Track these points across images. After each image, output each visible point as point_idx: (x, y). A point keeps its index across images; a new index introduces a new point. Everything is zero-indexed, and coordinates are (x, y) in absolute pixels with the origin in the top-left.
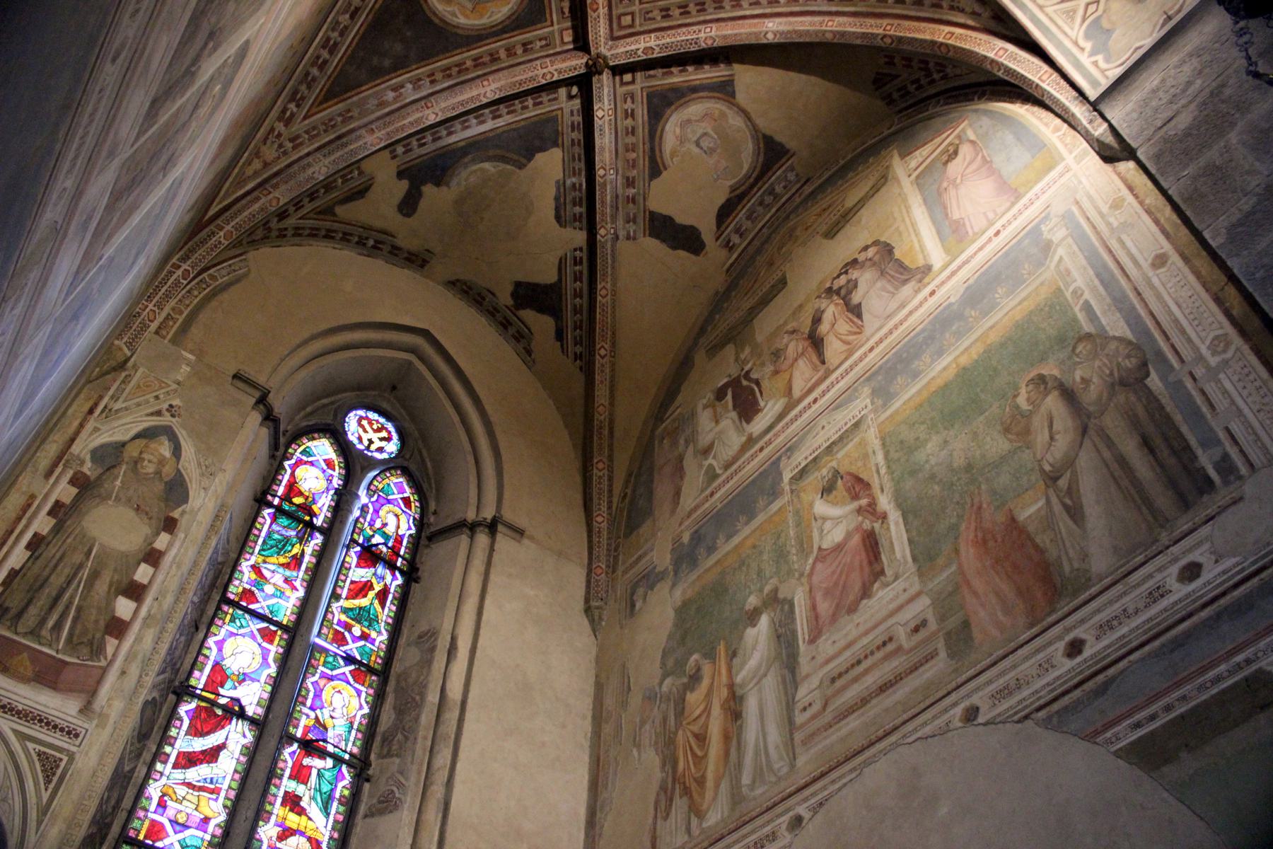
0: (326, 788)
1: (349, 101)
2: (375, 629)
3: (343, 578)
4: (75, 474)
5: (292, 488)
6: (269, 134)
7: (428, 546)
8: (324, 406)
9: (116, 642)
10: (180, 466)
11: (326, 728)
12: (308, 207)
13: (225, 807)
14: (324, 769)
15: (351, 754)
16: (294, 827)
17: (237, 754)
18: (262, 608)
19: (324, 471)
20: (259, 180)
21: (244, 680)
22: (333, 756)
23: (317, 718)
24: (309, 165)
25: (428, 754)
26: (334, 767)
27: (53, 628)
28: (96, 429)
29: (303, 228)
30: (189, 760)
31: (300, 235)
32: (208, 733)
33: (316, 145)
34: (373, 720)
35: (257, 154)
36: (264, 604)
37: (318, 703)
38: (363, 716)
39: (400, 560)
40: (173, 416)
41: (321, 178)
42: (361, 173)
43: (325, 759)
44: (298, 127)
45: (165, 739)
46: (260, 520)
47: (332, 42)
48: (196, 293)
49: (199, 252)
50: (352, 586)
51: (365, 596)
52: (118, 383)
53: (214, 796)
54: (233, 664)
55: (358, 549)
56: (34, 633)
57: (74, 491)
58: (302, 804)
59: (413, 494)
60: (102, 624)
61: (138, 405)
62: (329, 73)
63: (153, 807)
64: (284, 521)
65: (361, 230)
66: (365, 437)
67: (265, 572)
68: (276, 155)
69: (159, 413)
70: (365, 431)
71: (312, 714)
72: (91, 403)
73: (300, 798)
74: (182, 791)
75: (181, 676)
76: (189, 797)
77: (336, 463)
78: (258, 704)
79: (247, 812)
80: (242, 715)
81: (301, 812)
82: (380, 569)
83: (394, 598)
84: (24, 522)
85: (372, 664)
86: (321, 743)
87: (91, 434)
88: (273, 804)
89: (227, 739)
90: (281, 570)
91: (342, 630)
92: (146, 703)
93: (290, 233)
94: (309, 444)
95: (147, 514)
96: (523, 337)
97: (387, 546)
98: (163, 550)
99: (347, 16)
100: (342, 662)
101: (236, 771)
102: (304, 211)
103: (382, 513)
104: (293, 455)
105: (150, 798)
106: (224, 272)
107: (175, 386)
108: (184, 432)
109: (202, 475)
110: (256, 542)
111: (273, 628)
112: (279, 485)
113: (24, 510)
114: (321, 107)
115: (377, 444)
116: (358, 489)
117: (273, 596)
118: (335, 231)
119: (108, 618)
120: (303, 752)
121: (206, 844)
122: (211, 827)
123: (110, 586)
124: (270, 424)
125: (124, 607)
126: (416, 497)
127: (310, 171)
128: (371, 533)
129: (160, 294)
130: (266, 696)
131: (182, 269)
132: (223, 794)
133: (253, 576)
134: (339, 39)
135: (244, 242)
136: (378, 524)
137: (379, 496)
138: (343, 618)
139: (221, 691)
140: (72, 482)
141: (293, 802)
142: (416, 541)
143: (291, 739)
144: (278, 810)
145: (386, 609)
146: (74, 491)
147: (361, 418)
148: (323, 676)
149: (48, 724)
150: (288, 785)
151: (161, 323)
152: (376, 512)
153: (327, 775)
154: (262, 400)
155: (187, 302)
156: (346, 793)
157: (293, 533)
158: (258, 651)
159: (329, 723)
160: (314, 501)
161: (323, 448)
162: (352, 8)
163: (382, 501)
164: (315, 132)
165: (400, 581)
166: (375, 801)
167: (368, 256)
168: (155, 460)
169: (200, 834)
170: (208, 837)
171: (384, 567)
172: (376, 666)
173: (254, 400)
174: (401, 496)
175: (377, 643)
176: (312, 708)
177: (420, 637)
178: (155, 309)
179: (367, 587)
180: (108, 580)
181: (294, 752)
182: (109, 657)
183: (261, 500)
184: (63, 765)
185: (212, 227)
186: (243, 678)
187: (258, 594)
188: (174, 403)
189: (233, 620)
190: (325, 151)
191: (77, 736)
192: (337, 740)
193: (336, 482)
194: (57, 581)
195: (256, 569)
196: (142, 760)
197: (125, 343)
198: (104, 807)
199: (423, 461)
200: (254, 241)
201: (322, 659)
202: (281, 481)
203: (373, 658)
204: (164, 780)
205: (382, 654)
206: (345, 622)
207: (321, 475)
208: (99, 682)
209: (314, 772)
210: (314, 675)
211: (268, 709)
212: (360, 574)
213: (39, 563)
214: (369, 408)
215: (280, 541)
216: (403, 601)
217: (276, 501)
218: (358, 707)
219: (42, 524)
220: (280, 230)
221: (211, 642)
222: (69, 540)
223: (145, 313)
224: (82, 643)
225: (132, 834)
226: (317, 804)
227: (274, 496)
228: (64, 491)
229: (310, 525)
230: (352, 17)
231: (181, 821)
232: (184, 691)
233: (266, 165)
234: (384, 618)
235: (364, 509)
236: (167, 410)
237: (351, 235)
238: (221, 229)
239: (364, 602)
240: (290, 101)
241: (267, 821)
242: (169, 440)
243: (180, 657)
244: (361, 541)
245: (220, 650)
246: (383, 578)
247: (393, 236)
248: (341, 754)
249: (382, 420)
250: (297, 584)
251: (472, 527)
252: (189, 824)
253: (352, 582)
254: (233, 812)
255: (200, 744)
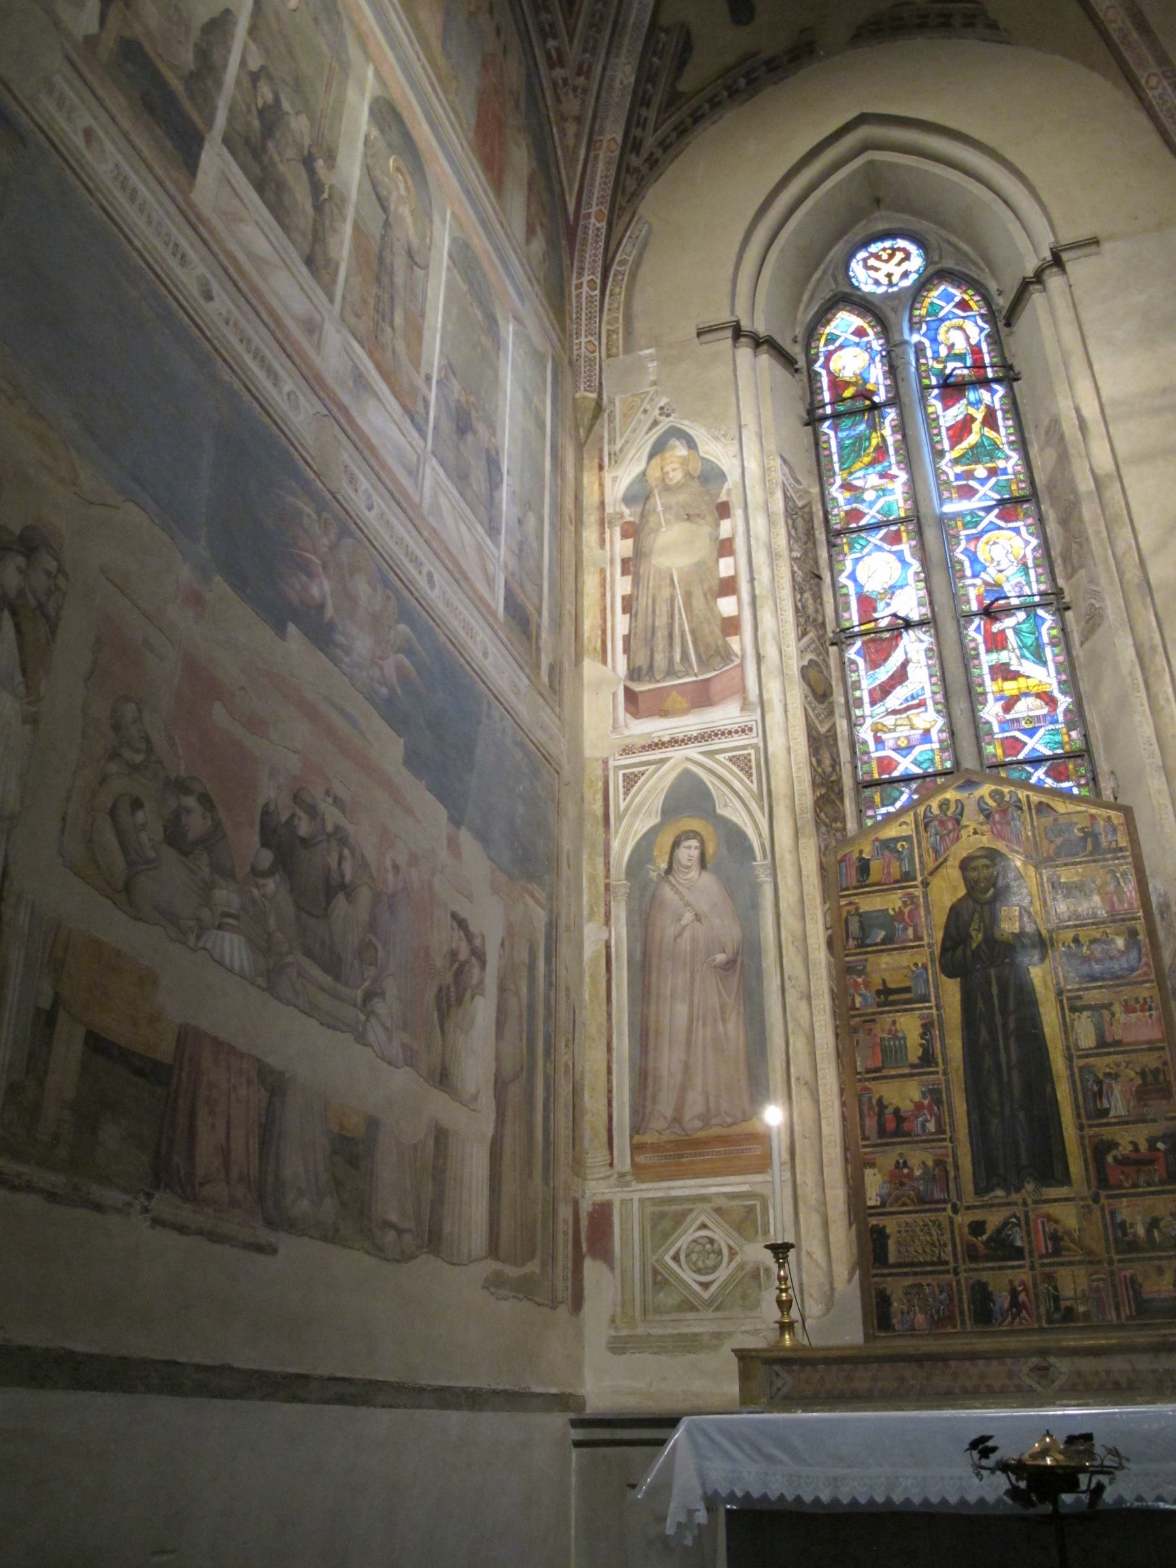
0: (1030, 640)
2: (999, 458)
3: (935, 431)
4: (622, 528)
5: (837, 385)
6: (555, 90)
7: (1011, 333)
8: (819, 281)
9: (737, 637)
10: (702, 454)
11: (1000, 586)
12: (651, 114)
13: (938, 712)
14: (1019, 624)
15: (1041, 594)
16: (1015, 692)
17: (923, 661)
18: (873, 517)
19: (857, 344)
20: (585, 140)
21: (893, 593)
22: (1018, 608)
23: (986, 583)
24: (612, 79)
25: (1108, 545)
26: (1028, 616)
27: (682, 660)
28: (615, 479)
29: (667, 136)
30: (883, 691)
31: (670, 145)
32: (886, 660)
33: (603, 55)
34: (1045, 545)
35: (563, 118)
36: (873, 512)
37: (978, 567)
38: (1034, 550)
39: (989, 370)
40: (668, 415)
41: (633, 79)
42: (667, 31)
43: (1013, 614)
44: (573, 54)
45: (848, 687)
46: (824, 438)
48: (617, 290)
49: (587, 256)
50: (951, 433)
51: (970, 432)
52: (606, 425)
53: (922, 709)
54: (873, 586)
55: (936, 392)
56: (671, 672)
57: (630, 542)
58: (1012, 668)
59: (965, 292)
60: (718, 631)
61: (634, 431)
63: (872, 746)
64: (846, 422)
65: (719, 82)
66: (881, 276)
67: (856, 483)
68: (579, 102)
69: (655, 423)
70: (876, 269)
71: (978, 581)
72: (596, 461)
73: (1007, 665)
74: (890, 721)
75: (830, 626)
76: (899, 722)
77: (866, 326)
78: (920, 604)
79: (960, 706)
80: (908, 625)
81: (1015, 676)
82: (972, 395)
83: (1004, 412)
84: (608, 595)
85: (1016, 494)
86: (1002, 602)
87: (613, 485)
88: (982, 685)
89: (906, 654)
90: (870, 470)
91: (964, 482)
92: (804, 671)
93: (659, 153)
94: (828, 330)
95: (699, 516)
96: (974, 16)
97: (966, 367)
98: (730, 536)
100: (982, 514)
101: (931, 676)
102: (651, 124)
103: (941, 337)
104: (817, 355)
105: (865, 743)
106: (629, 248)
107: (653, 388)
108: (686, 422)
109: (726, 445)
110: (831, 462)
111: (894, 528)
112: (822, 393)
113: (603, 585)
115: (897, 272)
116: (902, 334)
117: (878, 498)
118: (699, 107)
119: (719, 622)
120: (988, 621)
121: (937, 752)
122: (934, 735)
123: (705, 595)
124: (765, 347)
125: (727, 606)
126: (971, 292)
127: (617, 85)
128: (940, 366)
129: (584, 322)
130: (923, 593)
131: (585, 285)
132: (930, 703)
133: (847, 494)
135: (624, 204)
136: (943, 352)
137: (927, 323)
138: (959, 469)
139: (876, 615)
140: (625, 536)
141: (1003, 672)
142: (995, 339)
143: (969, 616)
144: (990, 686)
145: (1002, 430)
146: (630, 542)
147: (865, 260)
148: (969, 538)
149: (723, 734)
150: (987, 660)
151: (607, 344)
152: (934, 340)
153: (1024, 627)
154: (738, 333)
155: (616, 305)
156: (1054, 632)
157: (862, 427)
158: (893, 558)
159: (1001, 578)
160: (866, 382)
161: (845, 322)
163: (933, 325)
164: (591, 43)
165: (1000, 390)
166: (1083, 623)
167: (752, 96)
168: (677, 465)
169: (927, 747)
170: (936, 746)
171: (975, 389)
172: (1022, 493)
173: (730, 341)
174: (953, 304)
175: (1010, 470)
176: (975, 576)
177: (1047, 433)
178: (590, 338)
179: (969, 420)
180: (701, 595)
181: (979, 626)
182: (738, 652)
183: (813, 419)
184: (753, 757)
185: (582, 222)
186: (892, 590)
187: (862, 507)
188: (662, 404)
189: (851, 548)
190: (614, 50)
191: (751, 730)
192: (1017, 589)
193: (877, 345)
194: (662, 621)
195: (847, 486)
196: (837, 716)
197: (585, 390)
198: (819, 770)
199: (957, 249)
200: (633, 194)
201: (959, 524)
202: (821, 388)
203: (1014, 487)
204: (869, 721)
205: (1022, 477)
206: (963, 472)
207: (857, 350)
208: (743, 678)
209: (1010, 634)
210: (958, 544)
211: (931, 603)
212: (950, 416)
213: (640, 617)
214: (865, 244)
215: (853, 444)
216: (1014, 407)
217: (828, 410)
218: (1023, 545)
219: (623, 586)
220: (646, 161)
221: (843, 579)
222: (651, 585)
223: (583, 349)
224: (711, 656)
225: (867, 778)
226: (1027, 659)
227: (824, 406)
228: (623, 547)
229: (875, 407)
231: (903, 745)
232: (844, 637)
233: (579, 120)
234: (1004, 440)
235: (919, 349)
236: (661, 414)
237: (716, 95)
238: (588, 216)
239: (973, 439)
240: (545, 42)
241: (985, 703)
242: (678, 439)
243: (817, 611)
244: (934, 381)
245: (855, 580)
246: (980, 401)
247: (755, 54)
248: (1029, 600)
249: (888, 244)
250: (894, 470)
251: (1039, 277)
252: (913, 744)
253: (948, 429)
254: (947, 709)
255: (883, 674)
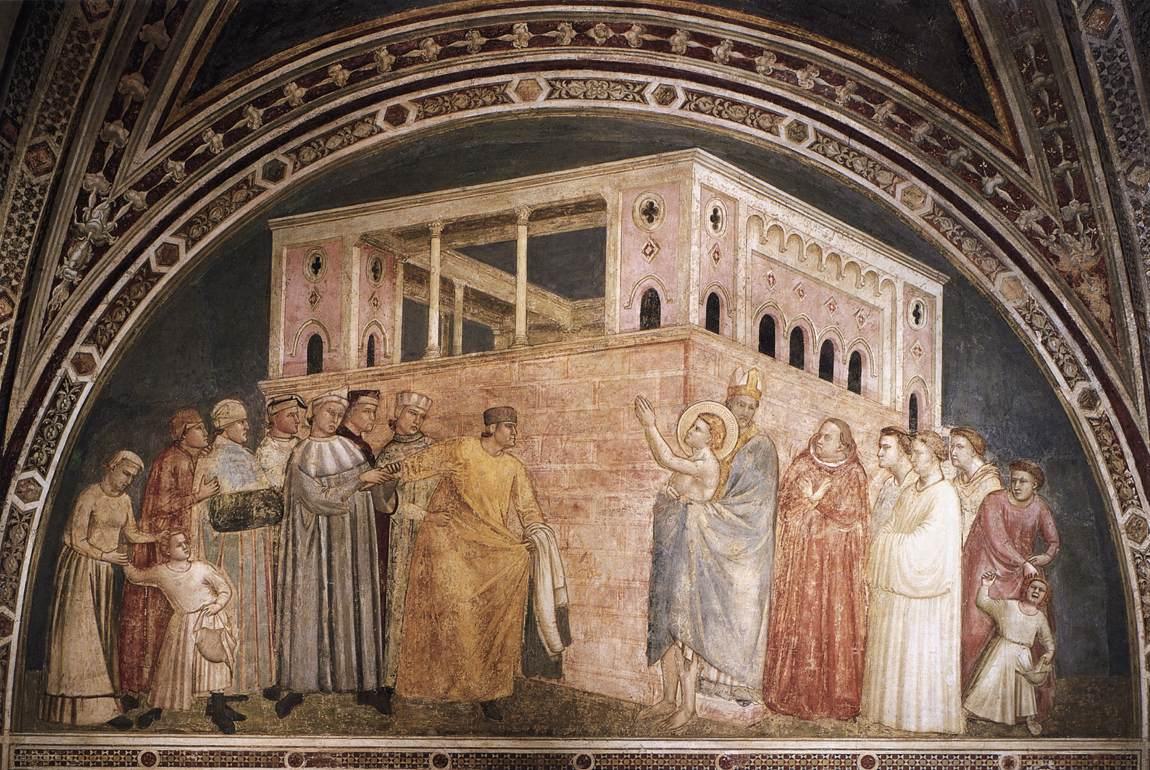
1: (995, 55)
6: (1038, 244)
35: (1071, 282)
47: (859, 98)
62: (924, 103)
99: (799, 74)
114: (1002, 121)
134: (850, 85)
162: (781, 67)
230: (800, 65)
233: (1101, 270)
240: (981, 187)
